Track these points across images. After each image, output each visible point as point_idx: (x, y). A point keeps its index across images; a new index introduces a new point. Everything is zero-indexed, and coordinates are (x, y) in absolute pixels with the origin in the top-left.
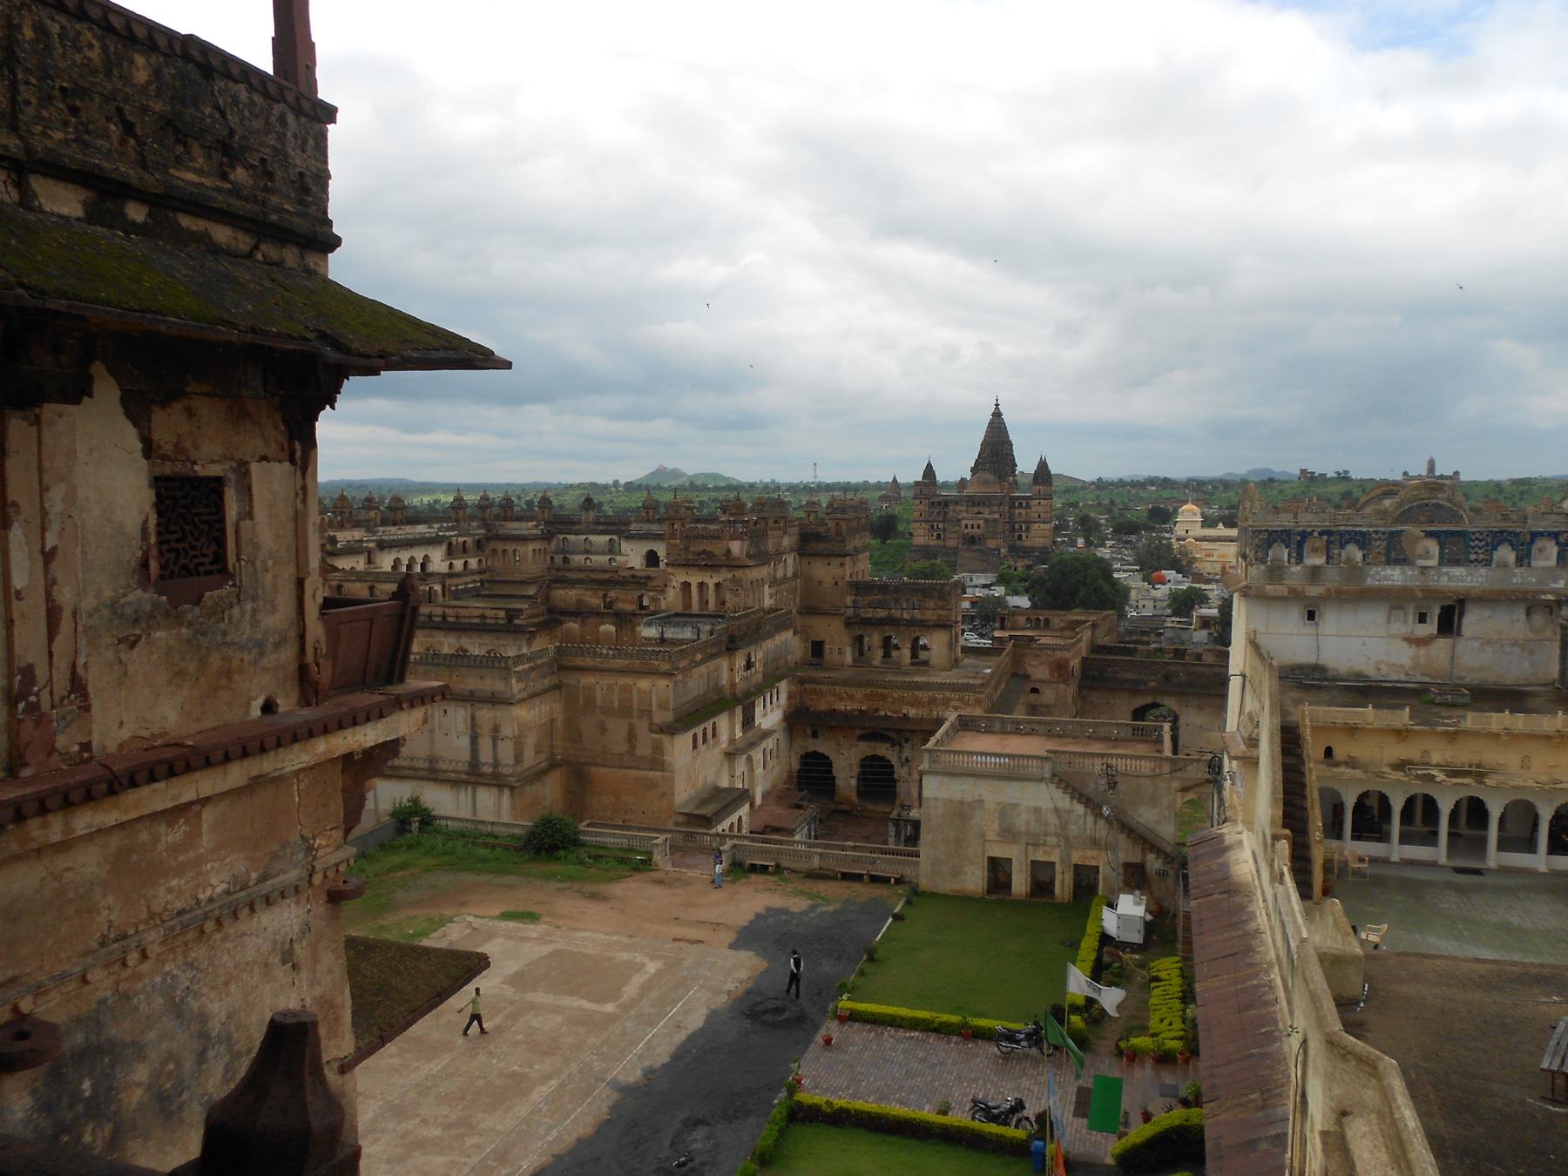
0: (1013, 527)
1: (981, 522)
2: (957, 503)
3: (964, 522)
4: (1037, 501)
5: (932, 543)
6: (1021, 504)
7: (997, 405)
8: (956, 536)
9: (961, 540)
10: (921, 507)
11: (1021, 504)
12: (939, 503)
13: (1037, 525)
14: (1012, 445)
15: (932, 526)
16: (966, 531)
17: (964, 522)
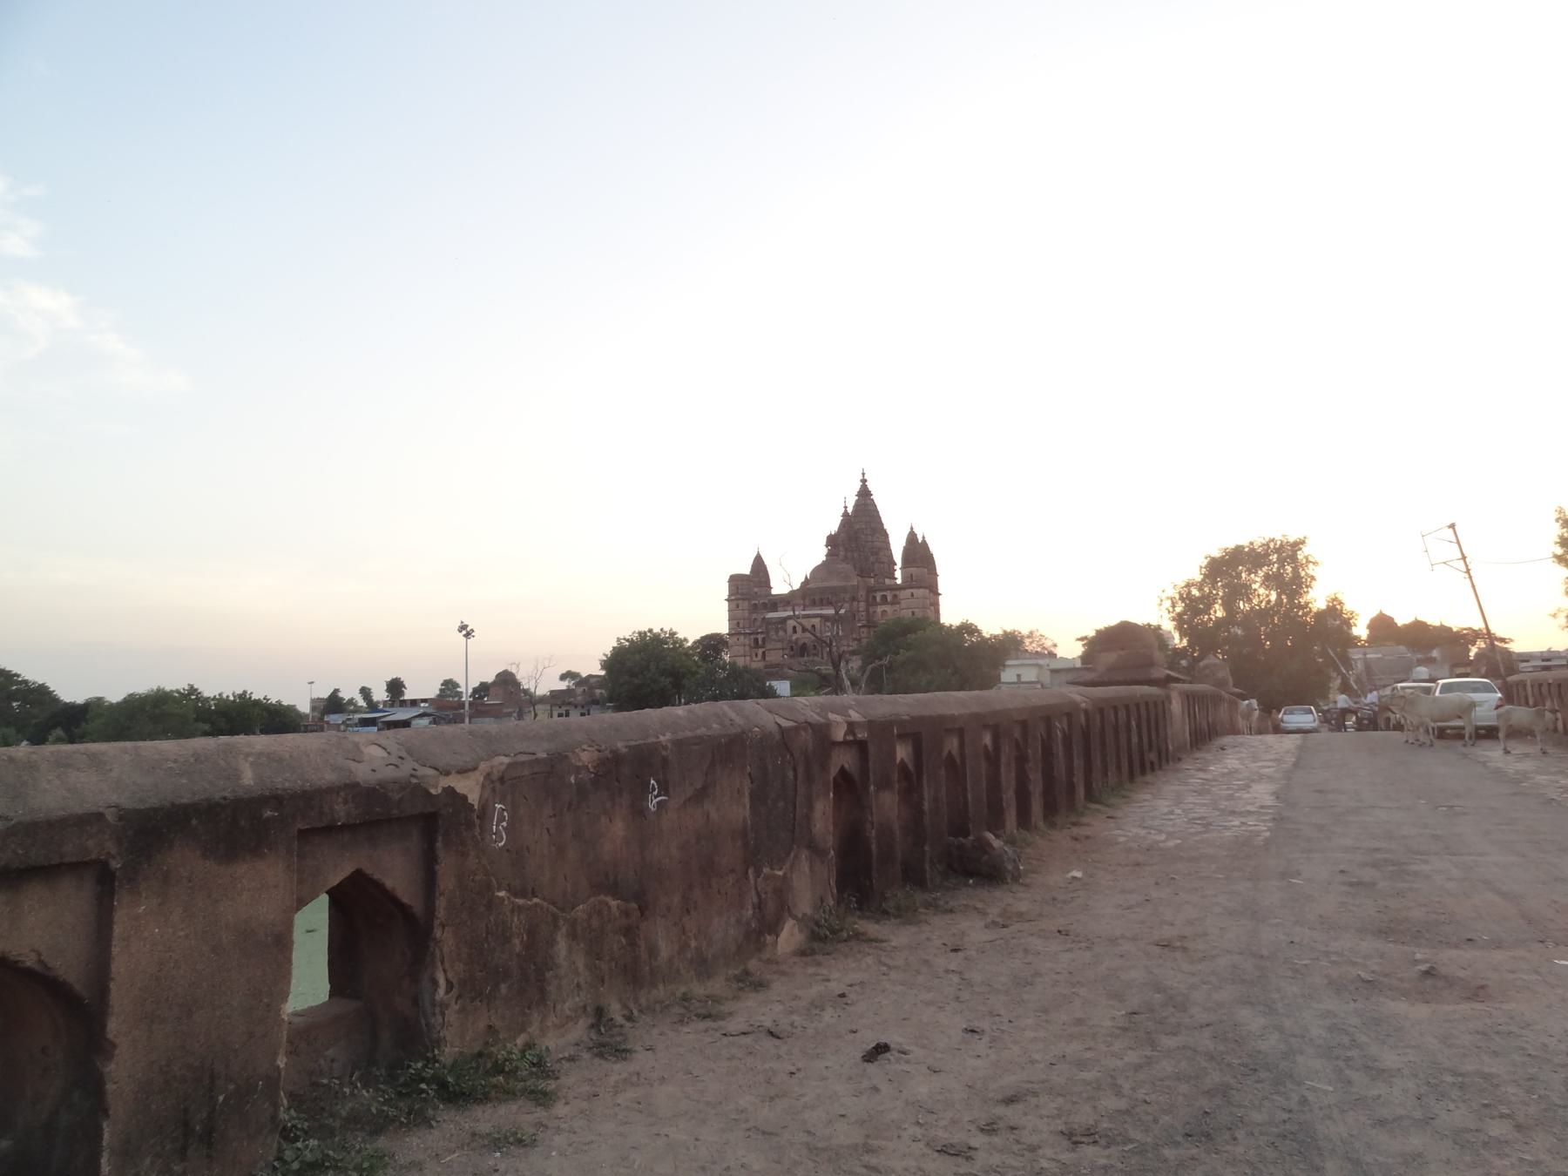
4: (909, 591)
5: (754, 665)
6: (884, 597)
7: (864, 481)
11: (884, 597)
12: (765, 605)
14: (886, 535)
15: (756, 640)
17: (791, 623)
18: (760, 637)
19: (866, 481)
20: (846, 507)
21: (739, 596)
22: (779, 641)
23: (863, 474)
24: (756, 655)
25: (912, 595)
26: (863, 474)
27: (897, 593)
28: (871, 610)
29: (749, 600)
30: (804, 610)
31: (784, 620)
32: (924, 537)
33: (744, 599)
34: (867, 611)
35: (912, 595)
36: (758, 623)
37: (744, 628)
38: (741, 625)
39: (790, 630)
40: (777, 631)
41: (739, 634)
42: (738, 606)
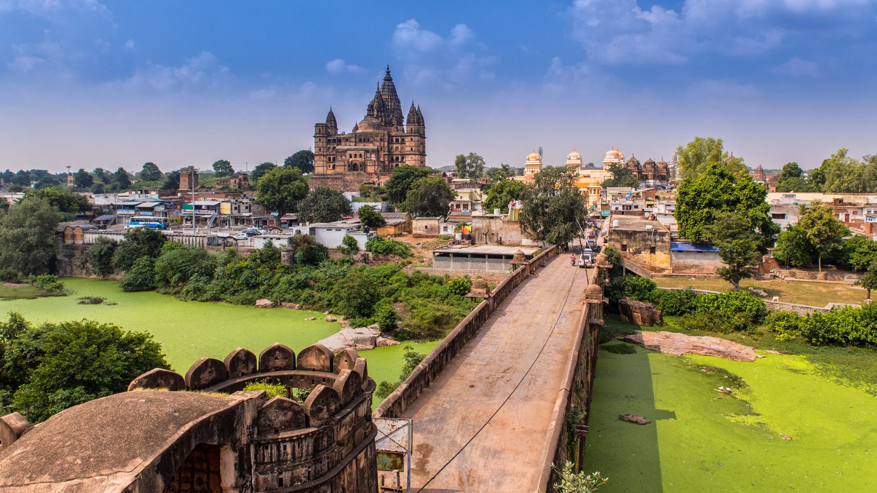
0: (392, 158)
1: (362, 152)
2: (347, 140)
3: (349, 152)
6: (397, 140)
7: (388, 73)
8: (342, 163)
9: (346, 167)
10: (321, 144)
11: (397, 140)
12: (334, 140)
13: (410, 156)
15: (330, 159)
16: (351, 160)
18: (332, 157)
19: (389, 72)
20: (378, 88)
21: (321, 135)
22: (342, 161)
23: (388, 68)
24: (330, 167)
25: (412, 139)
26: (388, 68)
27: (404, 138)
28: (390, 146)
29: (326, 137)
30: (356, 145)
31: (346, 151)
32: (419, 108)
33: (323, 137)
34: (388, 147)
35: (412, 139)
36: (331, 150)
37: (323, 152)
38: (322, 150)
39: (348, 156)
40: (341, 157)
41: (321, 155)
42: (320, 140)
